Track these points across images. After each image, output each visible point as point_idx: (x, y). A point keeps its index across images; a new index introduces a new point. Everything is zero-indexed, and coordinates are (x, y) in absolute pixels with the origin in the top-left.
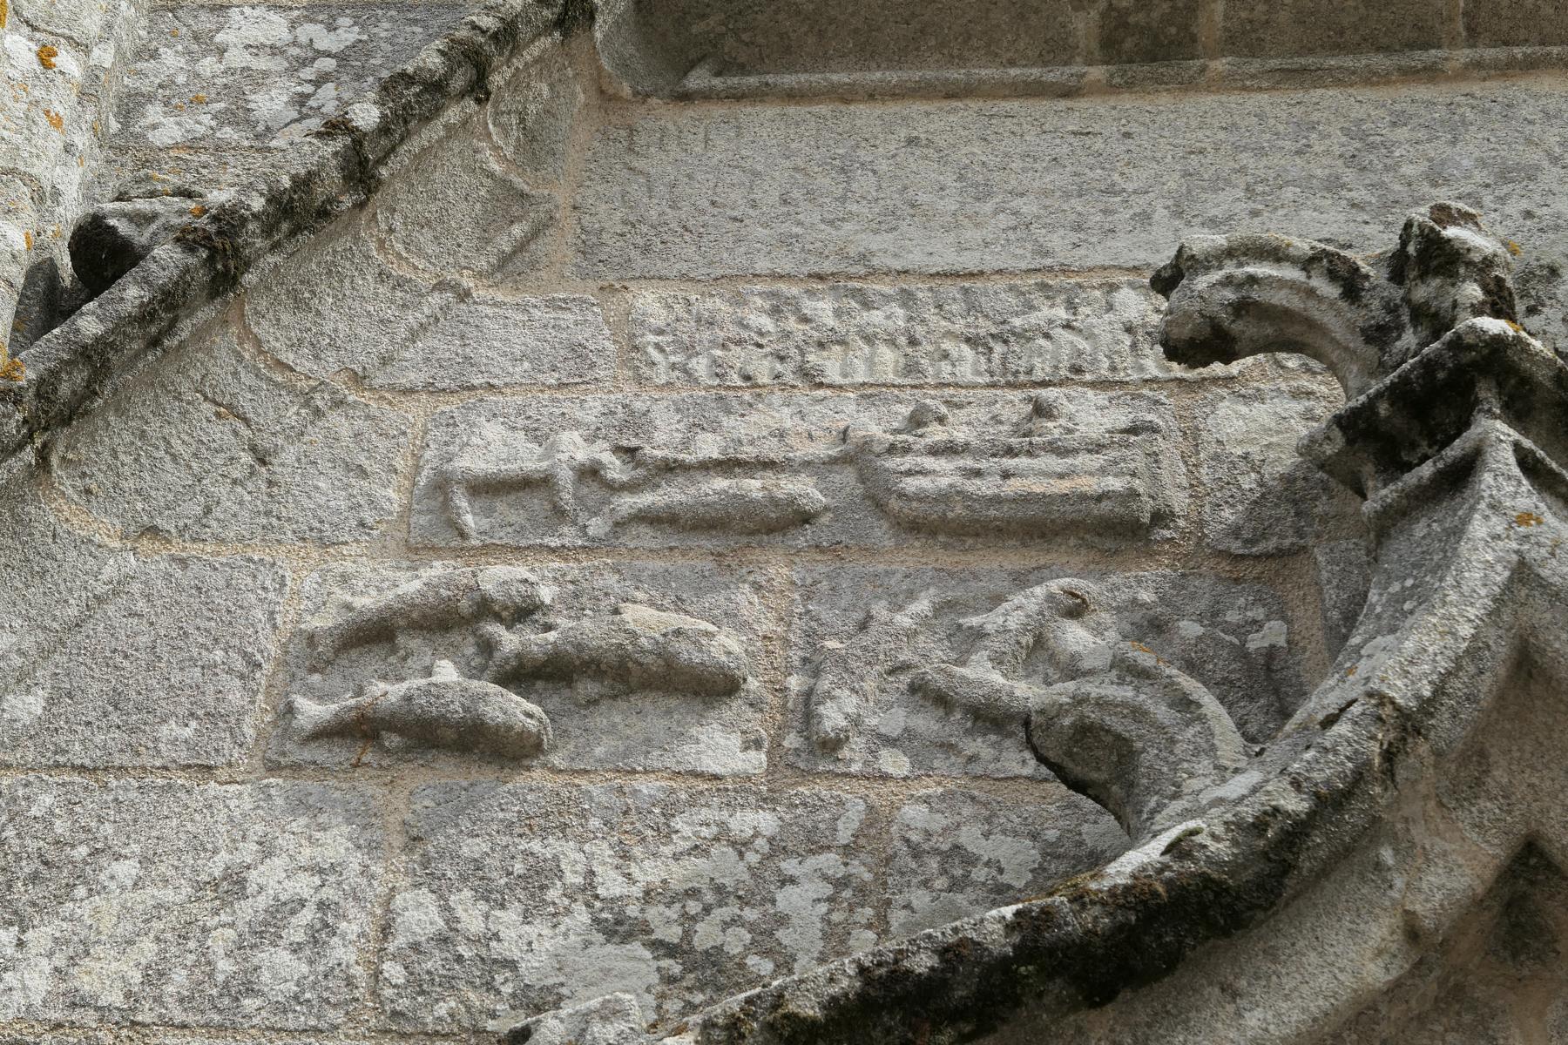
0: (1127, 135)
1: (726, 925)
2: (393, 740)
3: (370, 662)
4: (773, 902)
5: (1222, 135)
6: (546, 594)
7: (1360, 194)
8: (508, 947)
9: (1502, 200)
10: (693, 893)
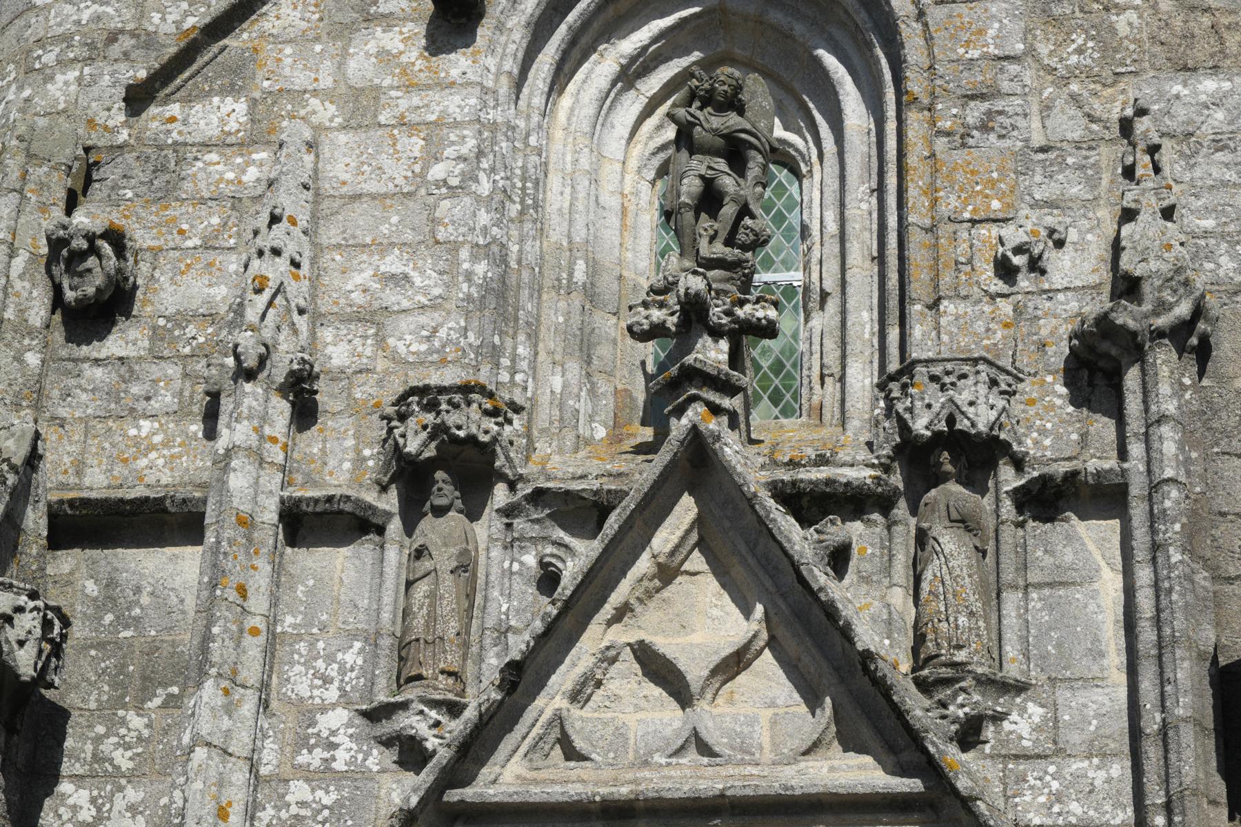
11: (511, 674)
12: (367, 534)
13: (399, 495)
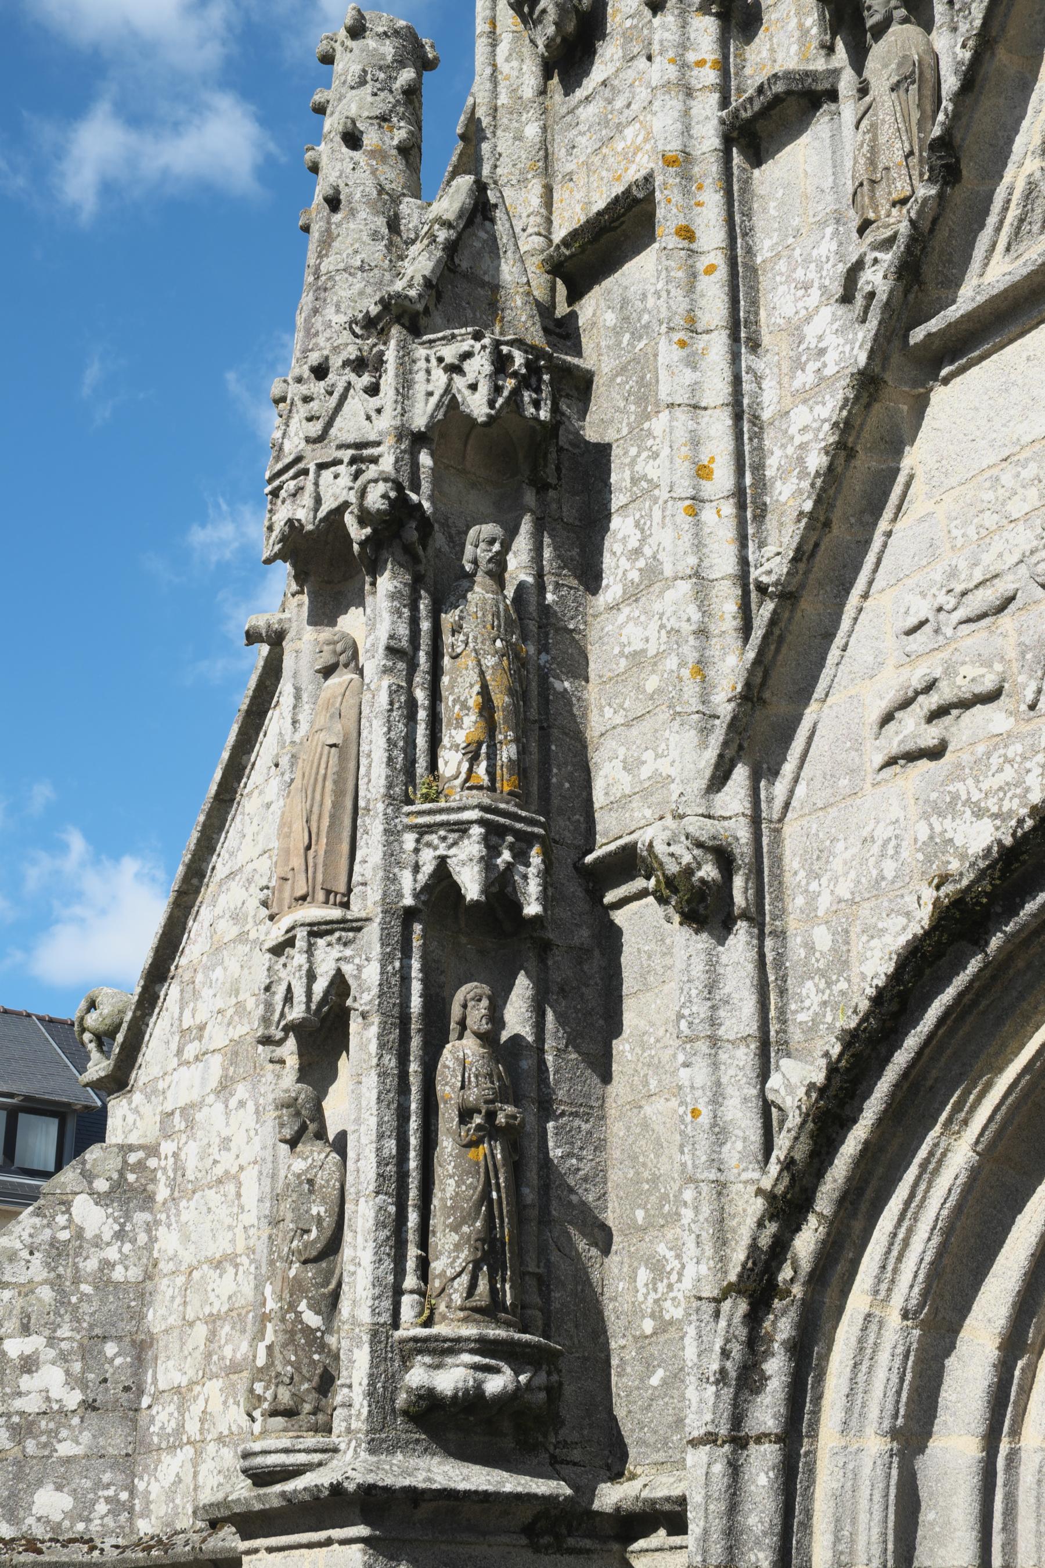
1: (1011, 798)
2: (902, 762)
3: (891, 726)
6: (937, 673)
10: (1001, 788)
11: (941, 158)
12: (820, 107)
13: (846, 45)
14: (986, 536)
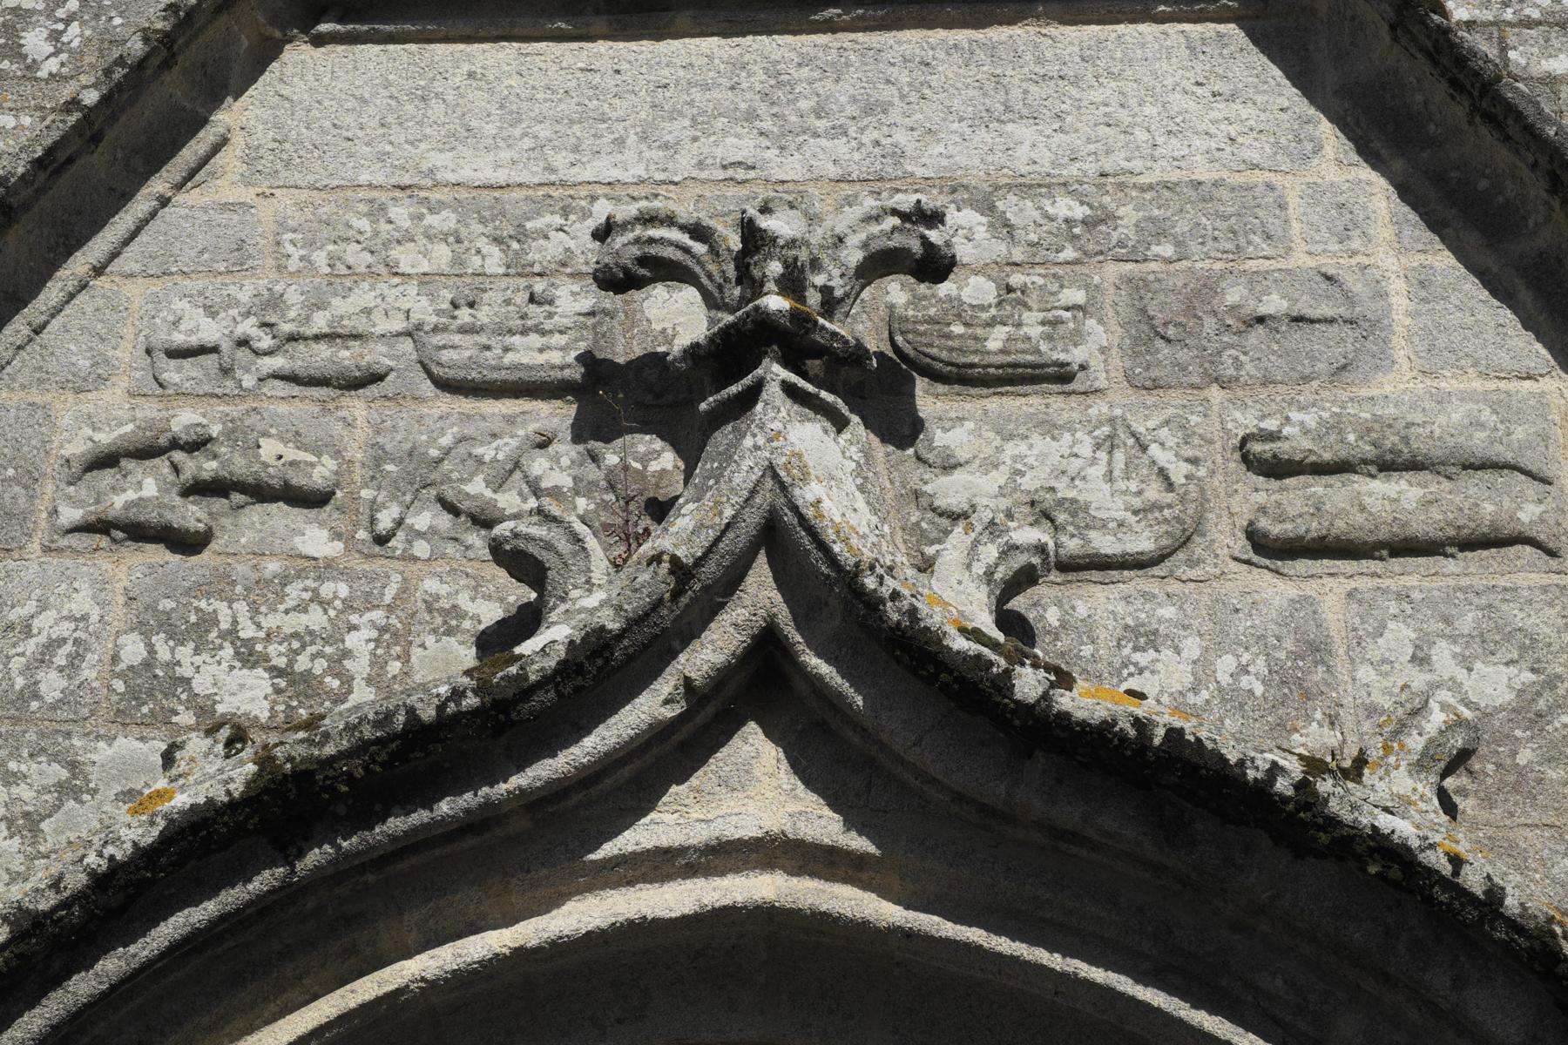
0: (618, 72)
1: (313, 657)
2: (119, 535)
3: (107, 477)
4: (343, 641)
5: (681, 73)
6: (215, 430)
7: (767, 125)
8: (185, 671)
9: (862, 130)
10: (295, 635)
14: (342, 277)
